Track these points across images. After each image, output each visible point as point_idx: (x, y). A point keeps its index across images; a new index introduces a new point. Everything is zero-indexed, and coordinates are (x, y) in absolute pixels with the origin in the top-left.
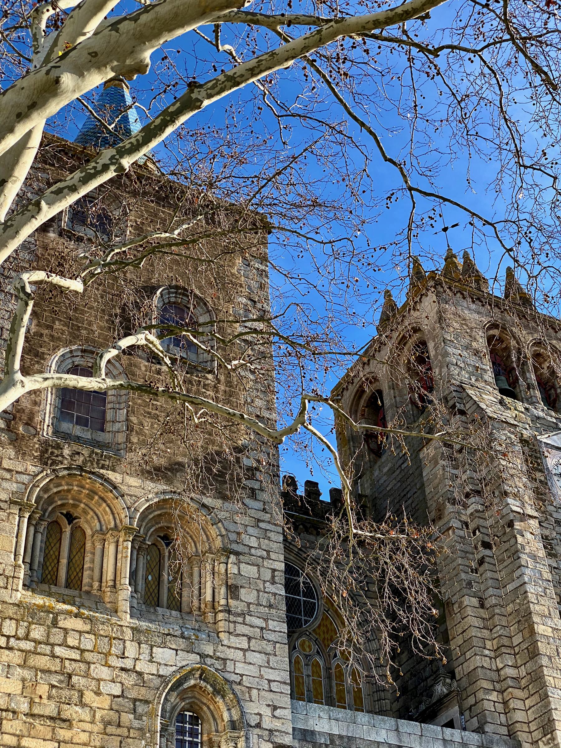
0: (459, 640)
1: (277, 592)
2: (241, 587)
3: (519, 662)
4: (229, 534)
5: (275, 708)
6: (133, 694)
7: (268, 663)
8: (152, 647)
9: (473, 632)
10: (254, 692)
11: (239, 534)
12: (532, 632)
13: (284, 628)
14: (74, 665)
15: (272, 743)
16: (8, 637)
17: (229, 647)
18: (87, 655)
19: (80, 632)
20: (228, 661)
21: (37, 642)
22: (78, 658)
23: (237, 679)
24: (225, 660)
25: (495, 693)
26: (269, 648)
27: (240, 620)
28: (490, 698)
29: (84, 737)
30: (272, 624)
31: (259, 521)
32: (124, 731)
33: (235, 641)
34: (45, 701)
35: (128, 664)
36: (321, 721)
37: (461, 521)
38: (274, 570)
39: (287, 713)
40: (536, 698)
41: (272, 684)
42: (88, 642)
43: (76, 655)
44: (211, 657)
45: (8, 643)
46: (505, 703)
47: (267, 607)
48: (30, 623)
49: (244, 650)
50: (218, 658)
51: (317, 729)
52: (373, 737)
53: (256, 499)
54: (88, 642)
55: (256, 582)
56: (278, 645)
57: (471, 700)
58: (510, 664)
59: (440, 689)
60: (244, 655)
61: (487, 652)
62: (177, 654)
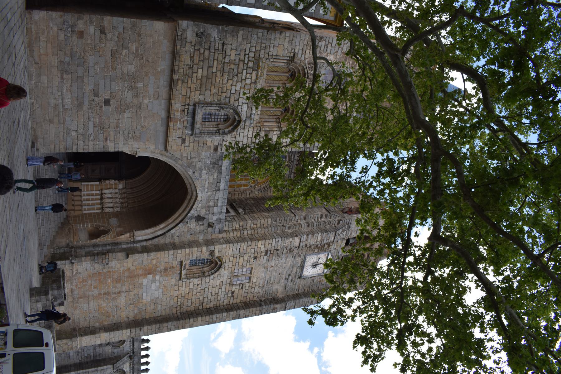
0: (256, 216)
3: (249, 236)
6: (232, 97)
8: (247, 103)
9: (259, 221)
12: (259, 240)
14: (241, 77)
16: (248, 54)
18: (243, 81)
19: (251, 79)
21: (247, 64)
22: (243, 78)
23: (238, 133)
24: (244, 129)
29: (218, 81)
32: (220, 94)
33: (250, 132)
34: (228, 68)
35: (241, 95)
40: (237, 239)
42: (248, 82)
43: (244, 77)
45: (247, 54)
46: (236, 230)
48: (253, 62)
50: (244, 127)
54: (248, 82)
57: (236, 219)
59: (240, 210)
61: (252, 225)
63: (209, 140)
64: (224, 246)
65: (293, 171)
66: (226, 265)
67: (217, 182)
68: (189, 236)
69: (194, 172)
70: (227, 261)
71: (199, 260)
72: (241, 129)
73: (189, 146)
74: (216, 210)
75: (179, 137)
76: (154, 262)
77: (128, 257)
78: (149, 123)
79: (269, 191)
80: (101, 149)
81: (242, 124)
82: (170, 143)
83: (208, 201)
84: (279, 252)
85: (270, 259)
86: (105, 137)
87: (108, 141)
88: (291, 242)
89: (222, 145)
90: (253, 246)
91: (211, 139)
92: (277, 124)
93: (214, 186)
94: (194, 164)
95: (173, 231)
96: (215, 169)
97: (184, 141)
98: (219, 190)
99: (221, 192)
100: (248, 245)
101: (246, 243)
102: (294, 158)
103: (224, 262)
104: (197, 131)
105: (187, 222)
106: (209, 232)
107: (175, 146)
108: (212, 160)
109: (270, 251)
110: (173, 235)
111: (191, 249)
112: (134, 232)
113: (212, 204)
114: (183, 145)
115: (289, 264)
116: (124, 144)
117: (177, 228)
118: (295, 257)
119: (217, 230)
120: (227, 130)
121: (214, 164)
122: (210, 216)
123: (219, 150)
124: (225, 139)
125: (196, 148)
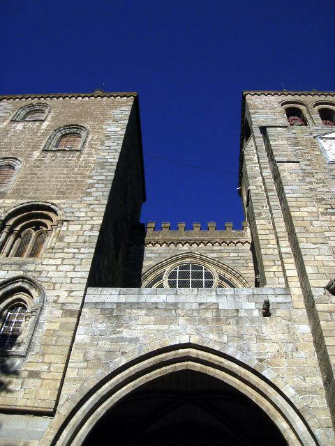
5: (72, 291)
10: (58, 285)
11: (73, 212)
13: (93, 251)
17: (47, 265)
20: (43, 272)
24: (40, 272)
30: (82, 251)
31: (90, 205)
39: (82, 293)
44: (32, 271)
49: (57, 265)
52: (154, 299)
58: (284, 245)
60: (57, 268)
61: (269, 246)
63: (45, 327)
64: (309, 270)
67: (156, 308)
68: (302, 354)
69: (123, 353)
73: (50, 364)
74: (225, 304)
75: (22, 384)
79: (246, 276)
82: (29, 403)
83: (204, 321)
84: (327, 196)
89: (64, 304)
90: (304, 224)
93: (165, 314)
95: (289, 392)
98: (175, 305)
99: (181, 299)
100: (303, 230)
102: (185, 250)
105: (261, 360)
107: (41, 391)
109: (327, 209)
110: (299, 391)
111: (325, 334)
114: (44, 375)
117: (279, 384)
119: (281, 299)
122: (242, 314)
124: (51, 300)
125: (57, 350)
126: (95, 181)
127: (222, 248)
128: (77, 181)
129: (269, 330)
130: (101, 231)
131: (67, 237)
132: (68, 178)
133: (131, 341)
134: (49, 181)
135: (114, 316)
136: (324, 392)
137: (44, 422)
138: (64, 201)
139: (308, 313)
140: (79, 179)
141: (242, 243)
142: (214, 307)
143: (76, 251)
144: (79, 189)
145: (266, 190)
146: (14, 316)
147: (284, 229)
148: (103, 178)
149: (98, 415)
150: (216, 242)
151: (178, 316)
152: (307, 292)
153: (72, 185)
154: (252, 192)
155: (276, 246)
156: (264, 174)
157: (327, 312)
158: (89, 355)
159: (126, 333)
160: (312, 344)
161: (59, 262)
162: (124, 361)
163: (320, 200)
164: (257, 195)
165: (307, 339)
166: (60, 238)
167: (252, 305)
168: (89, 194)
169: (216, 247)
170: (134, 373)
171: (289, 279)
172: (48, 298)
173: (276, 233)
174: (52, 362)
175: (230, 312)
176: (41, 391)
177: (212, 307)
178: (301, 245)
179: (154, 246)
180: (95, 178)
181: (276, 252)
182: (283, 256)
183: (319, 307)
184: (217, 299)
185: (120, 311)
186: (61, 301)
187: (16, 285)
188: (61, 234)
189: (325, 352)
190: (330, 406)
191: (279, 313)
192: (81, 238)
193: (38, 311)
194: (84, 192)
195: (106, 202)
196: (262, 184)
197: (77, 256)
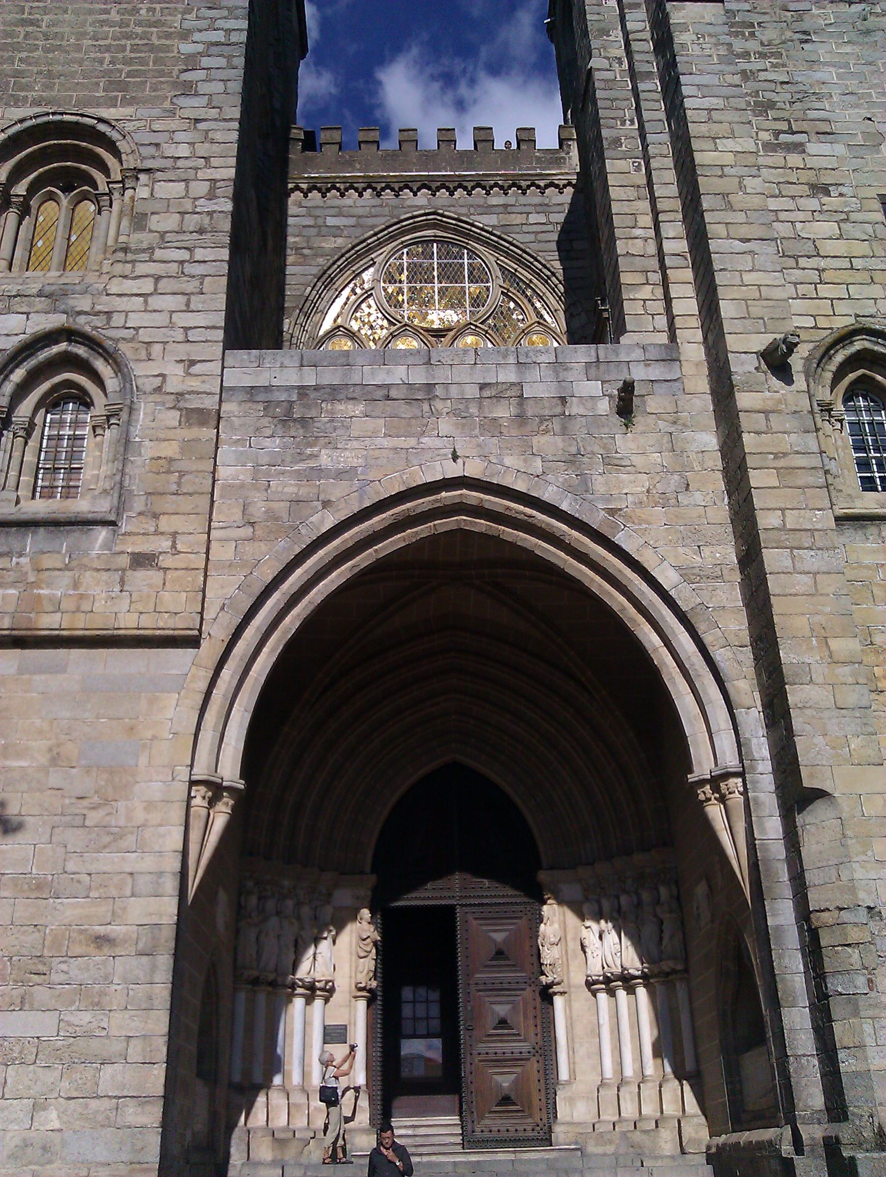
1: (216, 208)
2: (152, 213)
4: (142, 149)
5: (193, 363)
7: (188, 305)
10: (157, 349)
11: (157, 145)
13: (225, 254)
15: (180, 409)
20: (115, 316)
24: (109, 314)
25: (649, 288)
26: (191, 286)
27: (145, 256)
28: (638, 296)
30: (199, 254)
31: (197, 121)
33: (130, 286)
36: (285, 370)
37: (608, 58)
38: (215, 181)
39: (216, 367)
41: (190, 333)
47: (196, 232)
51: (275, 382)
53: (196, 95)
55: (180, 203)
56: (207, 279)
60: (146, 302)
61: (637, 232)
62: (28, 319)
63: (149, 450)
64: (727, 309)
65: (481, 201)
66: (872, 311)
67: (388, 398)
68: (698, 498)
69: (326, 504)
70: (841, 308)
71: (860, 447)
72: (108, 325)
73: (174, 535)
75: (122, 582)
76: (842, 646)
77: (820, 794)
78: (41, 732)
80: (153, 968)
81: (83, 323)
83: (492, 426)
84: (782, 97)
85: (825, 127)
86: (91, 949)
87: (116, 930)
88: (699, 36)
89: (181, 394)
91: (147, 443)
92: (116, 195)
93: (405, 410)
94: (281, 507)
95: (667, 578)
96: (313, 413)
97: (141, 560)
98: (430, 387)
99: (441, 375)
101: (708, 217)
103: (852, 320)
104: (103, 507)
105: (612, 512)
106: (671, 408)
107: (166, 596)
108: (268, 432)
109: (777, 133)
111: (750, 461)
112: (691, 777)
113: (504, 412)
114: (166, 561)
115: (848, 49)
116: (141, 848)
117: (647, 559)
118: (805, 33)
119: (656, 372)
120: (112, 383)
121: (287, 420)
122: (574, 408)
123: (210, 403)
124: (150, 384)
126: (200, 48)
127: (510, 199)
128: (152, 48)
129: (632, 445)
130: (237, 198)
131: (155, 218)
132: (127, 36)
133: (341, 474)
134: (78, 47)
135: (295, 420)
136: (737, 577)
137: (185, 655)
138: (128, 111)
139: (715, 405)
140: (155, 41)
141: (557, 186)
142: (514, 392)
143: (185, 255)
144: (162, 74)
145: (633, 73)
146: (61, 423)
147: (674, 190)
148: (219, 36)
149: (285, 632)
150: (496, 185)
151: (436, 414)
152: (716, 360)
153: (143, 62)
154: (597, 75)
155: (652, 233)
156: (630, 26)
157: (759, 412)
158: (251, 510)
159: (325, 459)
160: (719, 476)
161: (147, 286)
162: (330, 521)
163: (764, 107)
164: (610, 84)
165: (710, 464)
166: (139, 221)
167: (594, 388)
168: (188, 90)
169: (496, 199)
170: (350, 544)
171: (678, 323)
172: (140, 381)
173: (653, 200)
174: (176, 533)
175: (547, 405)
176: (166, 596)
177: (508, 394)
178: (713, 245)
179: (342, 195)
180: (197, 36)
181: (652, 249)
182: (668, 262)
183: (743, 400)
184: (520, 372)
185: (305, 406)
186: (170, 387)
187: (55, 349)
188: (139, 208)
189: (748, 499)
190: (747, 605)
191: (653, 404)
192: (192, 222)
193: (124, 415)
194: (175, 84)
195: (236, 113)
196: (621, 52)
197: (189, 269)
